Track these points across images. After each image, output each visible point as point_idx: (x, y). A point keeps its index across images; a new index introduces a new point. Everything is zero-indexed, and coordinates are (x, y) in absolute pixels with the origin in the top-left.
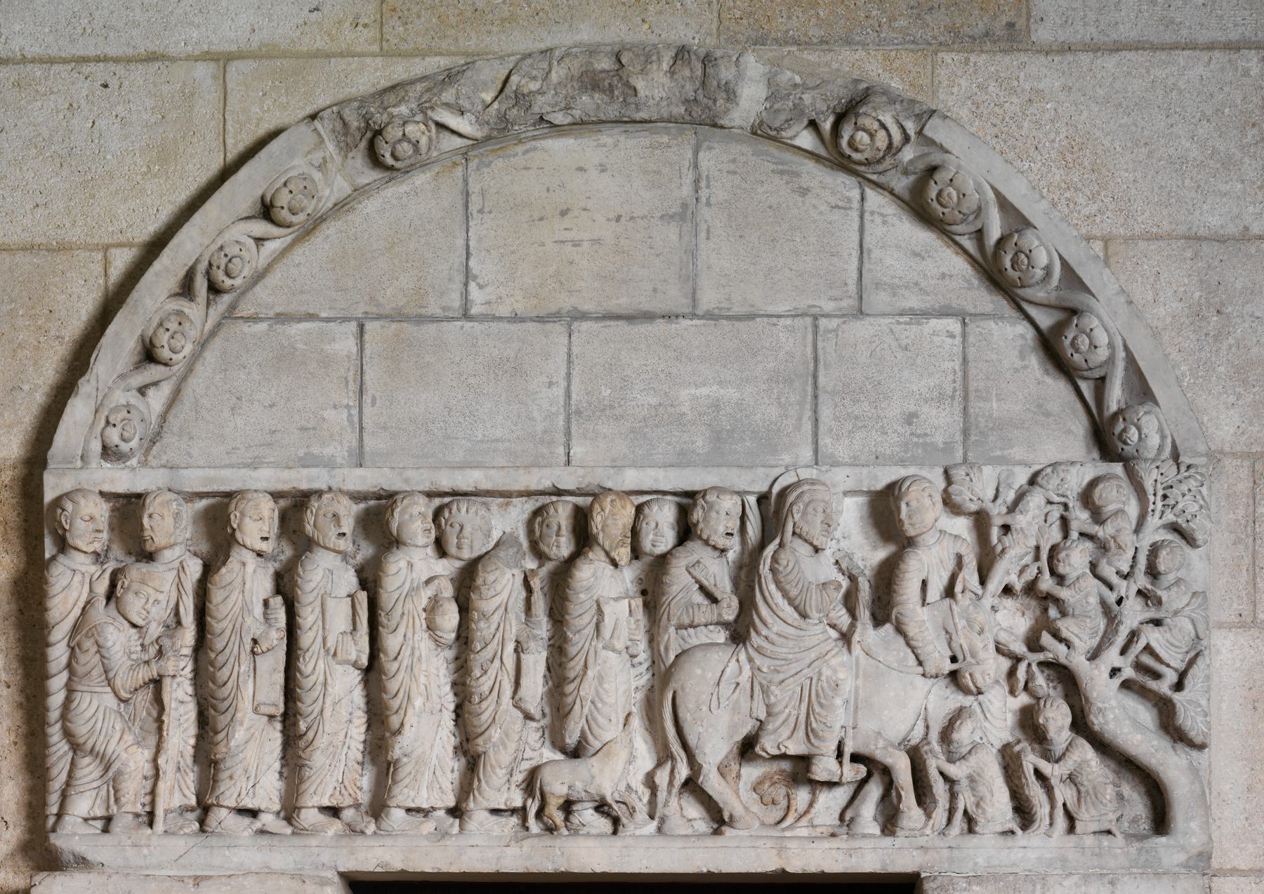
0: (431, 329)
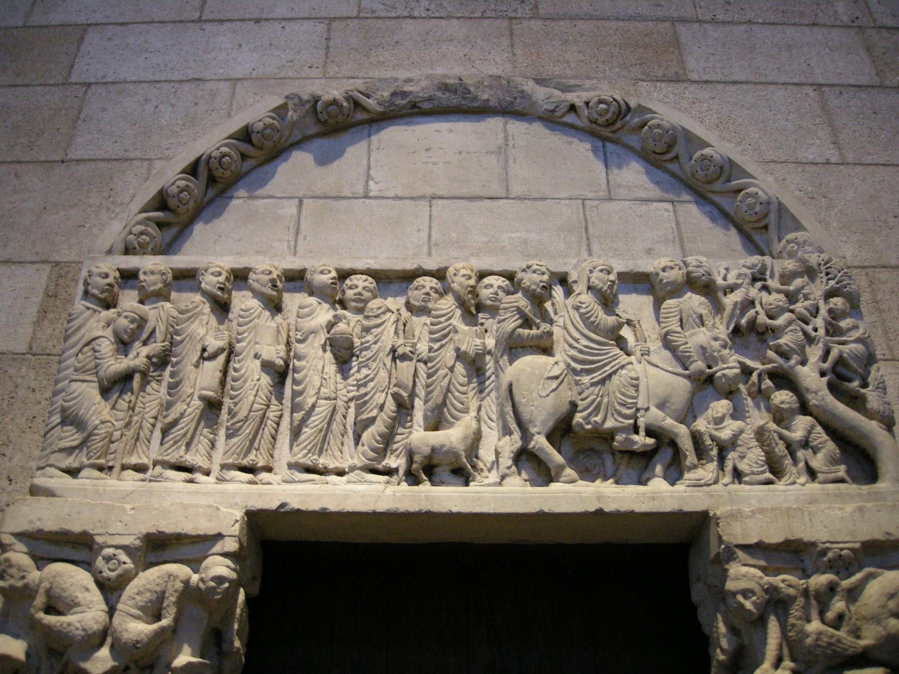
0: (344, 203)
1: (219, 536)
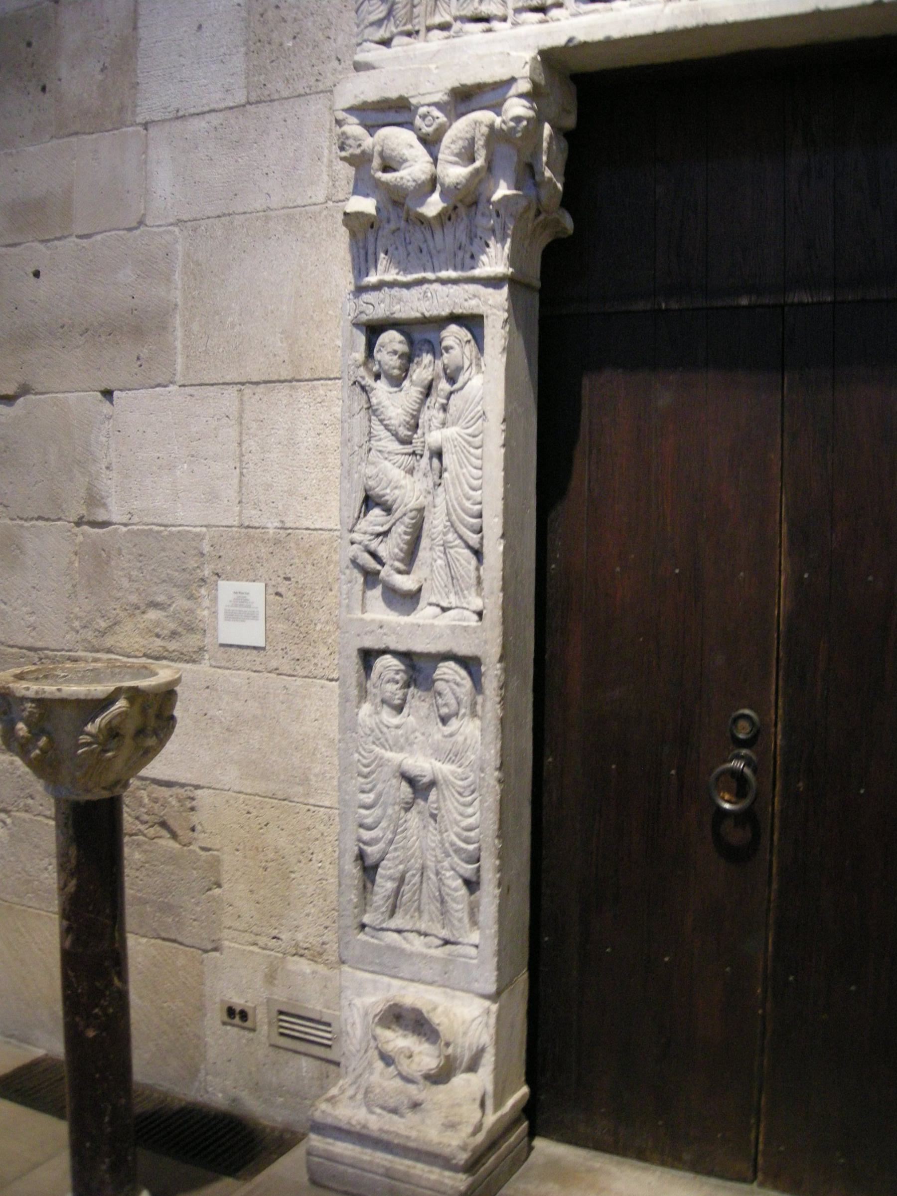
1: (513, 80)
